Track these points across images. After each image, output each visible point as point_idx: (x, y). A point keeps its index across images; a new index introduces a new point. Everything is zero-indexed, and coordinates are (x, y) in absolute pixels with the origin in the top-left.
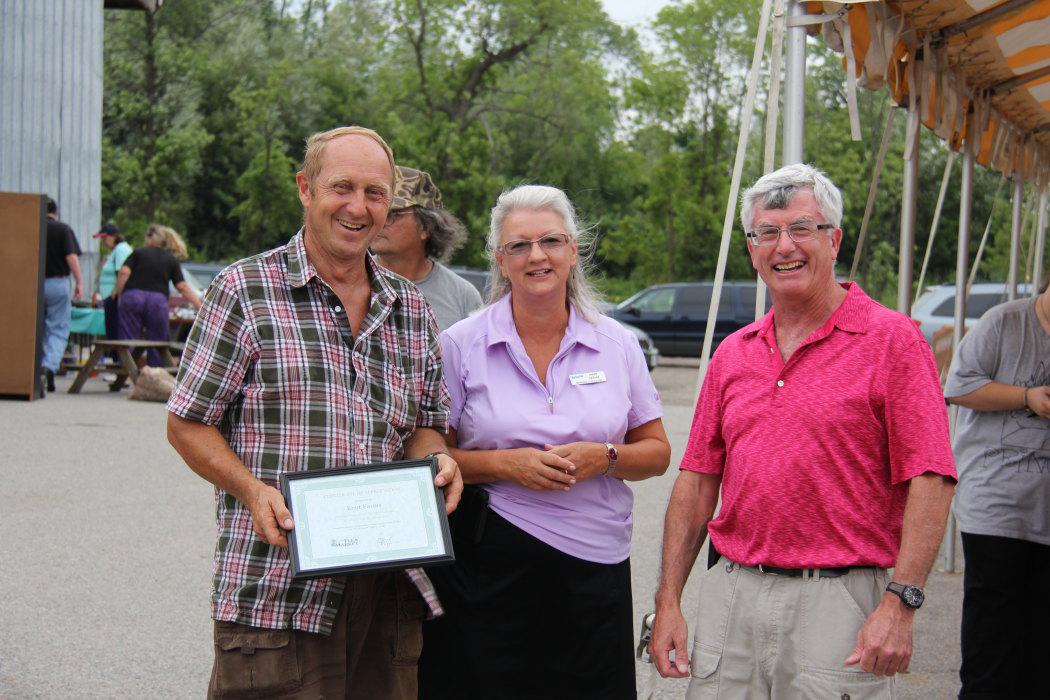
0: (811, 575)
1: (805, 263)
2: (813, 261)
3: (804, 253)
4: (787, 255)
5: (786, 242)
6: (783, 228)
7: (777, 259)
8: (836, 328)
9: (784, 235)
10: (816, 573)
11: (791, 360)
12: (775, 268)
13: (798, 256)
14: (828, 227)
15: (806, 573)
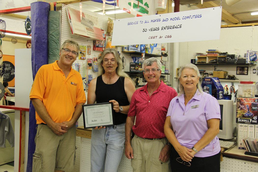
0: (155, 139)
1: (155, 77)
2: (156, 76)
3: (155, 75)
4: (151, 75)
5: (151, 73)
6: (151, 70)
7: (149, 76)
8: (159, 90)
9: (151, 71)
10: (156, 139)
11: (151, 96)
12: (149, 78)
13: (153, 76)
14: (159, 70)
15: (154, 139)
